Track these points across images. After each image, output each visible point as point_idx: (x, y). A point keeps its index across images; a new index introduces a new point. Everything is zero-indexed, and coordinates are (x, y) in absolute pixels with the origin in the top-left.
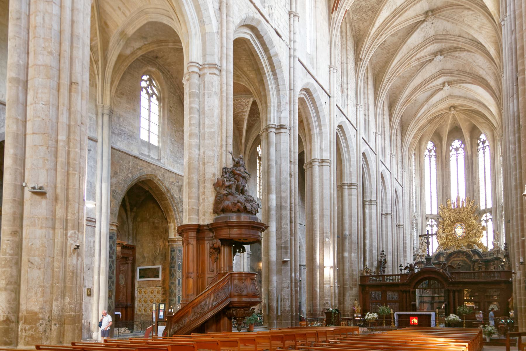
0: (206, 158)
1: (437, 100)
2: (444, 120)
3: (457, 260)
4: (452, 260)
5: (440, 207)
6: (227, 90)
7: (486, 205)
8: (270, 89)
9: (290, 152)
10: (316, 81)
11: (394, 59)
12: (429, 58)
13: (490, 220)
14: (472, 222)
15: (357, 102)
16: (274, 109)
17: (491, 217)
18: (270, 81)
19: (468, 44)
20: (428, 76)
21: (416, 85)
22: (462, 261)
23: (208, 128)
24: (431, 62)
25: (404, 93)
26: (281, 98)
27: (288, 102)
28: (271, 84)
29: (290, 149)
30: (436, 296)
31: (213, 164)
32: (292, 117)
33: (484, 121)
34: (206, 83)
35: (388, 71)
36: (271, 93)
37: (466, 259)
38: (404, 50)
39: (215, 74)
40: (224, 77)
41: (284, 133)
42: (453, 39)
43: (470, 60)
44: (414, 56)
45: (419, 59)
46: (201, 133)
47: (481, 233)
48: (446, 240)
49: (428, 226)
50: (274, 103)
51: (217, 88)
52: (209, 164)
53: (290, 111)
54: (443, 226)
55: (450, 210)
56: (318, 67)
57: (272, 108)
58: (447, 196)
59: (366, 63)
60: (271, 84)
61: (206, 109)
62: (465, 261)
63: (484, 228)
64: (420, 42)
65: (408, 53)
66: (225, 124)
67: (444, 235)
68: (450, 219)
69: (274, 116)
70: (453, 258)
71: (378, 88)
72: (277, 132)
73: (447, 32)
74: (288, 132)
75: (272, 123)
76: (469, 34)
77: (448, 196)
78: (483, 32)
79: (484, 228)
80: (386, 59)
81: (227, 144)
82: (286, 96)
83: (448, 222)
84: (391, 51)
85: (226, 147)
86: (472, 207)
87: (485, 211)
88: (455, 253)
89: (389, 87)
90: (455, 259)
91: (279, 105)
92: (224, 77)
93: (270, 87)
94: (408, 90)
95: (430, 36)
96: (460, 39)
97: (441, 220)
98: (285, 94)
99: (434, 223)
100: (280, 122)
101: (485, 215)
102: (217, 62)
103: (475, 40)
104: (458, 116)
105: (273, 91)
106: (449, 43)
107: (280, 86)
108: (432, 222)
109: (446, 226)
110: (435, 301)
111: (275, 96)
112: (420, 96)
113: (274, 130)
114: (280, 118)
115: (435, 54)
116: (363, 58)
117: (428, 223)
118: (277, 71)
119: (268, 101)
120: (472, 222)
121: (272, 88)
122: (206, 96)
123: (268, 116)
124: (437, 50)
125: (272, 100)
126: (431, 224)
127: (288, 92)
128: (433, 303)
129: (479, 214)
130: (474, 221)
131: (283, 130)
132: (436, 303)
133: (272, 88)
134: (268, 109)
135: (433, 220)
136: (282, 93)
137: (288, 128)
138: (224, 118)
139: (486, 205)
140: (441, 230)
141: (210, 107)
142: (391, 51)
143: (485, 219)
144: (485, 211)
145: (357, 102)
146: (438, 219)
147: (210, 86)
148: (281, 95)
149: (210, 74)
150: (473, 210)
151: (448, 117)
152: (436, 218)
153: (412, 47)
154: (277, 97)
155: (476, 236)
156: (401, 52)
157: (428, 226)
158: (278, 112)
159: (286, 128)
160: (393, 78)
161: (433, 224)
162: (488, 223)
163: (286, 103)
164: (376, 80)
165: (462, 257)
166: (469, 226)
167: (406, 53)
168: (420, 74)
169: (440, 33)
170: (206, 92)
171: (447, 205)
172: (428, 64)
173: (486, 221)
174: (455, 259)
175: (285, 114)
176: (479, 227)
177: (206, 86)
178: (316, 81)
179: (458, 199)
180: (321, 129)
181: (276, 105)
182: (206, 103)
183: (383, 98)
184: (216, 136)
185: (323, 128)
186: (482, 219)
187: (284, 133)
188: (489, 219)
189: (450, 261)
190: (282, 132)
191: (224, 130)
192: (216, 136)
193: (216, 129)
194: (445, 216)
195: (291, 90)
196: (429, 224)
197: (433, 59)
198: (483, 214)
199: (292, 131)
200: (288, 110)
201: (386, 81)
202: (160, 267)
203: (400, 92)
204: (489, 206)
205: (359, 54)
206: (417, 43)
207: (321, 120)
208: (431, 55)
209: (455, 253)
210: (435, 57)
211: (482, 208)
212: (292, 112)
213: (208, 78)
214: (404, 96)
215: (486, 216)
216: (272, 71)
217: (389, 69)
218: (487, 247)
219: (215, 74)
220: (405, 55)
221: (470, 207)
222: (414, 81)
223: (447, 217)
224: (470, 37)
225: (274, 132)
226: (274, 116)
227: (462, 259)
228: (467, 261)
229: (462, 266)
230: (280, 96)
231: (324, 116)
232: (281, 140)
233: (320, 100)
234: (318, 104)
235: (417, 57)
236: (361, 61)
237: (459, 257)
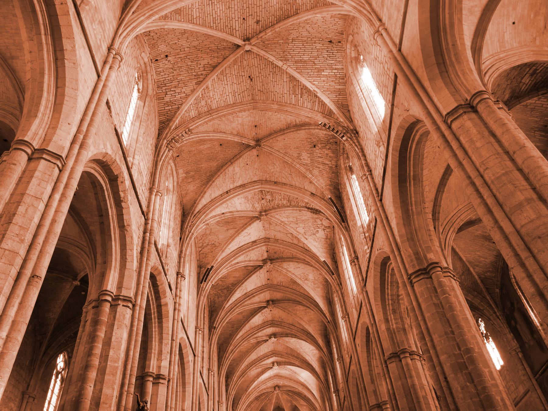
0: (102, 397)
1: (266, 378)
2: (269, 399)
6: (138, 325)
8: (154, 336)
9: (166, 407)
10: (188, 338)
11: (238, 334)
12: (265, 338)
15: (210, 367)
16: (154, 357)
18: (155, 328)
19: (300, 332)
20: (262, 354)
21: (251, 361)
23: (111, 361)
24: (266, 342)
25: (241, 366)
26: (163, 346)
27: (169, 352)
28: (155, 331)
29: (167, 403)
31: (110, 407)
32: (172, 368)
33: (305, 404)
34: (118, 313)
35: (232, 343)
36: (154, 339)
38: (247, 328)
39: (128, 307)
40: (138, 312)
41: (163, 384)
42: (288, 326)
43: (298, 346)
44: (255, 334)
45: (256, 338)
46: (101, 366)
50: (155, 350)
51: (127, 321)
52: (105, 406)
53: (170, 362)
56: (189, 325)
57: (153, 355)
59: (218, 332)
60: (155, 331)
61: (113, 340)
64: (260, 323)
65: (249, 331)
66: (131, 360)
69: (153, 364)
71: (222, 357)
72: (155, 381)
73: (282, 319)
74: (166, 383)
75: (151, 371)
76: (300, 324)
78: (311, 325)
80: (231, 332)
81: (129, 384)
82: (168, 345)
84: (235, 326)
85: (128, 387)
89: (231, 357)
91: (160, 353)
92: (138, 312)
93: (154, 333)
94: (244, 364)
95: (268, 320)
96: (293, 327)
98: (168, 343)
100: (159, 371)
102: (132, 295)
103: (305, 330)
104: (282, 396)
105: (155, 338)
106: (284, 329)
107: (164, 335)
111: (157, 344)
112: (253, 372)
113: (151, 379)
114: (159, 367)
115: (270, 336)
116: (217, 326)
118: (164, 320)
119: (149, 347)
121: (155, 335)
122: (115, 327)
123: (147, 363)
124: (271, 333)
125: (153, 347)
127: (170, 342)
131: (161, 381)
133: (155, 335)
134: (148, 355)
136: (164, 341)
137: (167, 380)
138: (131, 353)
141: (118, 338)
142: (235, 326)
145: (210, 367)
147: (122, 317)
148: (163, 344)
149: (123, 306)
151: (272, 396)
153: (253, 326)
154: (159, 345)
156: (244, 329)
158: (158, 360)
159: (165, 379)
160: (236, 350)
163: (168, 352)
164: (220, 349)
167: (248, 330)
168: (255, 351)
169: (276, 319)
170: (116, 322)
172: (263, 343)
175: (165, 363)
177: (117, 316)
178: (188, 338)
180: (185, 388)
181: (156, 352)
182: (114, 334)
184: (119, 373)
185: (187, 386)
187: (163, 384)
190: (161, 383)
191: (129, 367)
192: (119, 373)
193: (120, 364)
195: (172, 340)
197: (268, 340)
199: (171, 383)
200: (169, 360)
201: (229, 351)
203: (237, 364)
205: (213, 323)
206: (257, 324)
207: (186, 377)
208: (267, 336)
210: (270, 338)
212: (173, 363)
213: (120, 309)
214: (240, 370)
216: (158, 319)
217: (233, 341)
219: (128, 307)
220: (247, 332)
222: (250, 357)
224: (301, 328)
225: (152, 381)
226: (153, 364)
230: (162, 345)
231: (189, 374)
232: (158, 391)
233: (188, 357)
234: (185, 360)
235: (255, 336)
236: (214, 329)
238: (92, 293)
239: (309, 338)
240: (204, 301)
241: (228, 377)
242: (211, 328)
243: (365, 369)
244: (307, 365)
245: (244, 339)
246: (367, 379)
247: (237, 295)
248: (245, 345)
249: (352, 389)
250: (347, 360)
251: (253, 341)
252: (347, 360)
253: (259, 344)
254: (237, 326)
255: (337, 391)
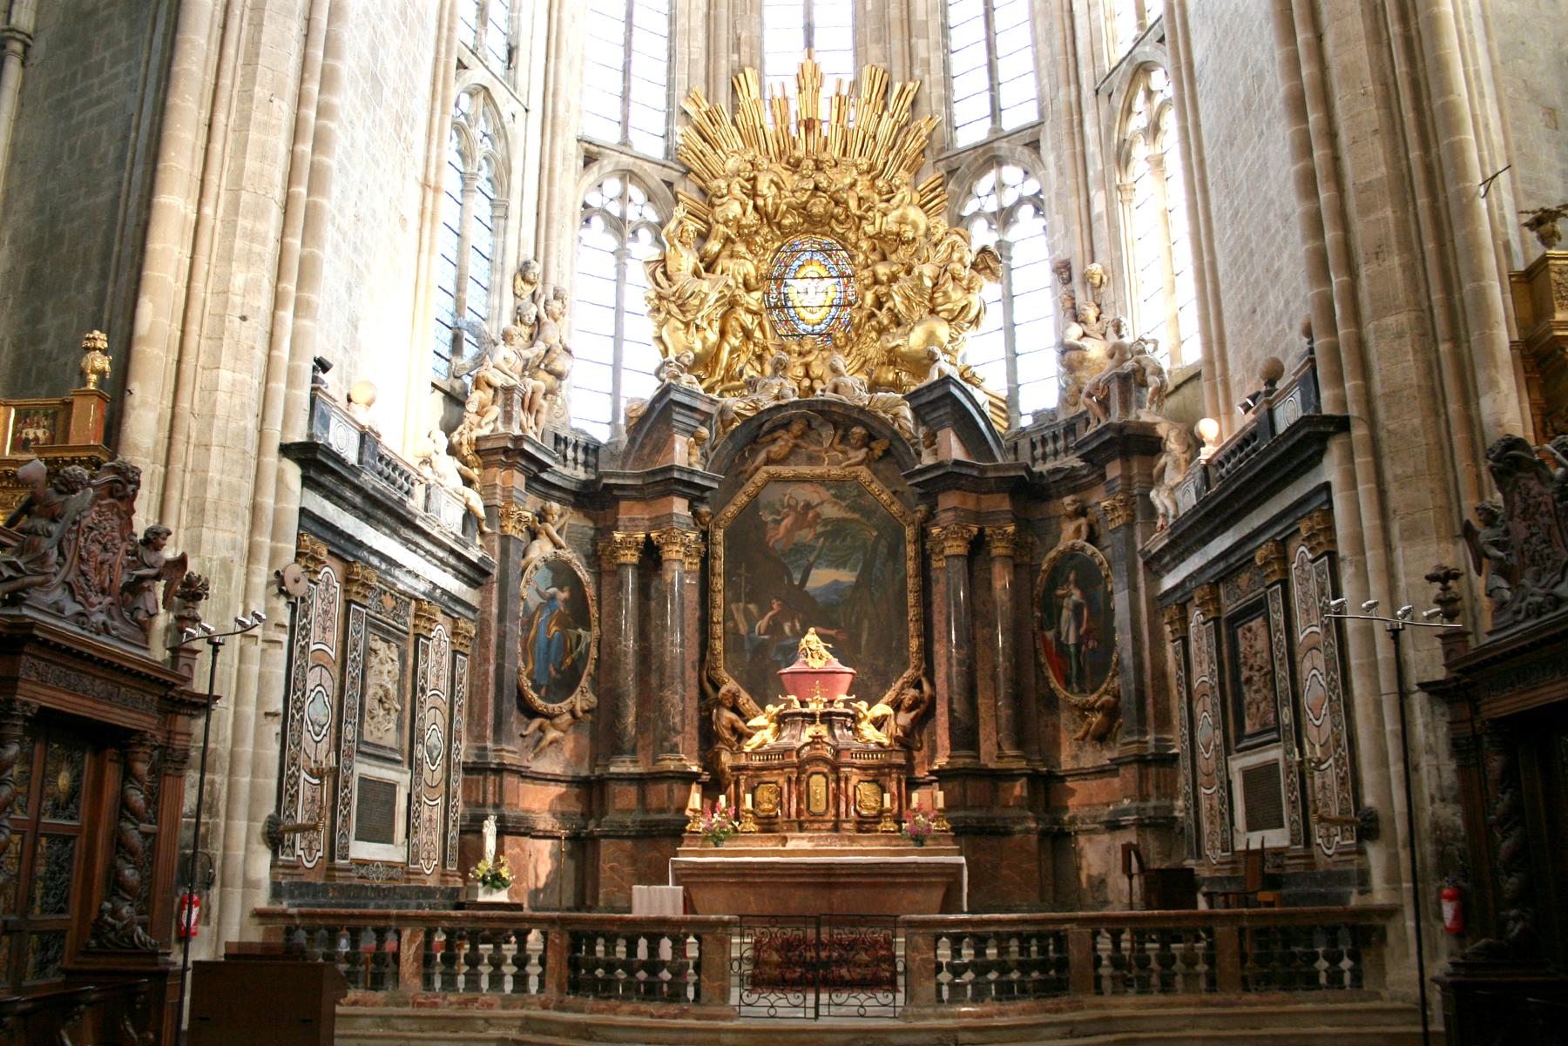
3: (799, 480)
4: (760, 477)
5: (691, 109)
7: (995, 112)
13: (1027, 211)
14: (902, 221)
17: (1031, 187)
22: (838, 486)
30: (620, 778)
37: (864, 473)
47: (969, 290)
48: (723, 333)
49: (597, 222)
54: (703, 237)
55: (752, 137)
58: (737, 47)
62: (862, 490)
63: (988, 262)
67: (710, 288)
68: (753, 193)
70: (769, 462)
77: (744, 49)
79: (988, 262)
83: (734, 209)
86: (903, 128)
87: (988, 157)
88: (786, 425)
90: (786, 471)
97: (687, 190)
99: (639, 209)
101: (985, 183)
108: (623, 197)
109: (728, 240)
110: (612, 816)
117: (595, 200)
120: (902, 221)
126: (615, 209)
128: (594, 840)
129: (951, 172)
130: (915, 214)
132: (616, 835)
135: (635, 192)
139: (995, 112)
140: (686, 261)
143: (991, 205)
144: (988, 157)
146: (670, 185)
150: (912, 146)
152: (655, 176)
155: (932, 312)
157: (597, 222)
161: (632, 214)
162: (1012, 235)
165: (833, 463)
166: (886, 244)
171: (735, 108)
173: (1005, 217)
174: (786, 471)
176: (953, 247)
179: (808, 79)
186: (970, 207)
188: (1021, 201)
189: (750, 488)
194: (717, 168)
196: (604, 213)
198: (980, 172)
204: (1019, 115)
209: (786, 425)
211: (971, 133)
215: (1000, 186)
218: (1010, 404)
221: (887, 125)
223: (738, 173)
227: (835, 471)
228: (875, 487)
229: (837, 530)
237: (813, 460)
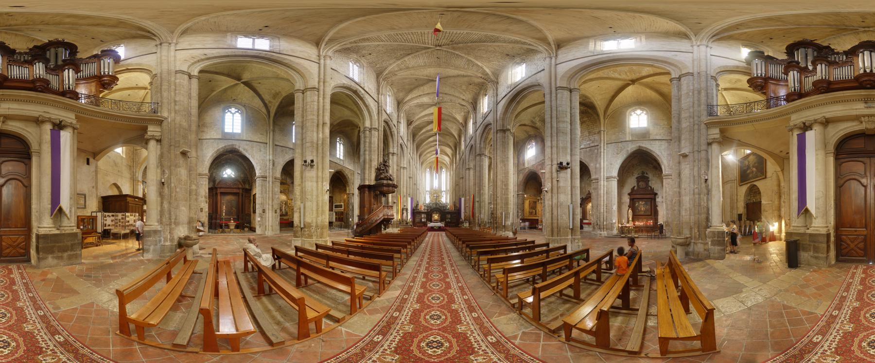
183: (418, 154)
202: (343, 204)
238: (362, 129)
239: (449, 147)
240: (410, 131)
241: (420, 156)
242: (414, 141)
243: (467, 158)
244: (447, 155)
245: (426, 145)
246: (467, 160)
247: (424, 130)
248: (426, 147)
249: (461, 163)
250: (461, 154)
251: (429, 146)
252: (461, 154)
253: (431, 147)
254: (423, 141)
255: (456, 163)
